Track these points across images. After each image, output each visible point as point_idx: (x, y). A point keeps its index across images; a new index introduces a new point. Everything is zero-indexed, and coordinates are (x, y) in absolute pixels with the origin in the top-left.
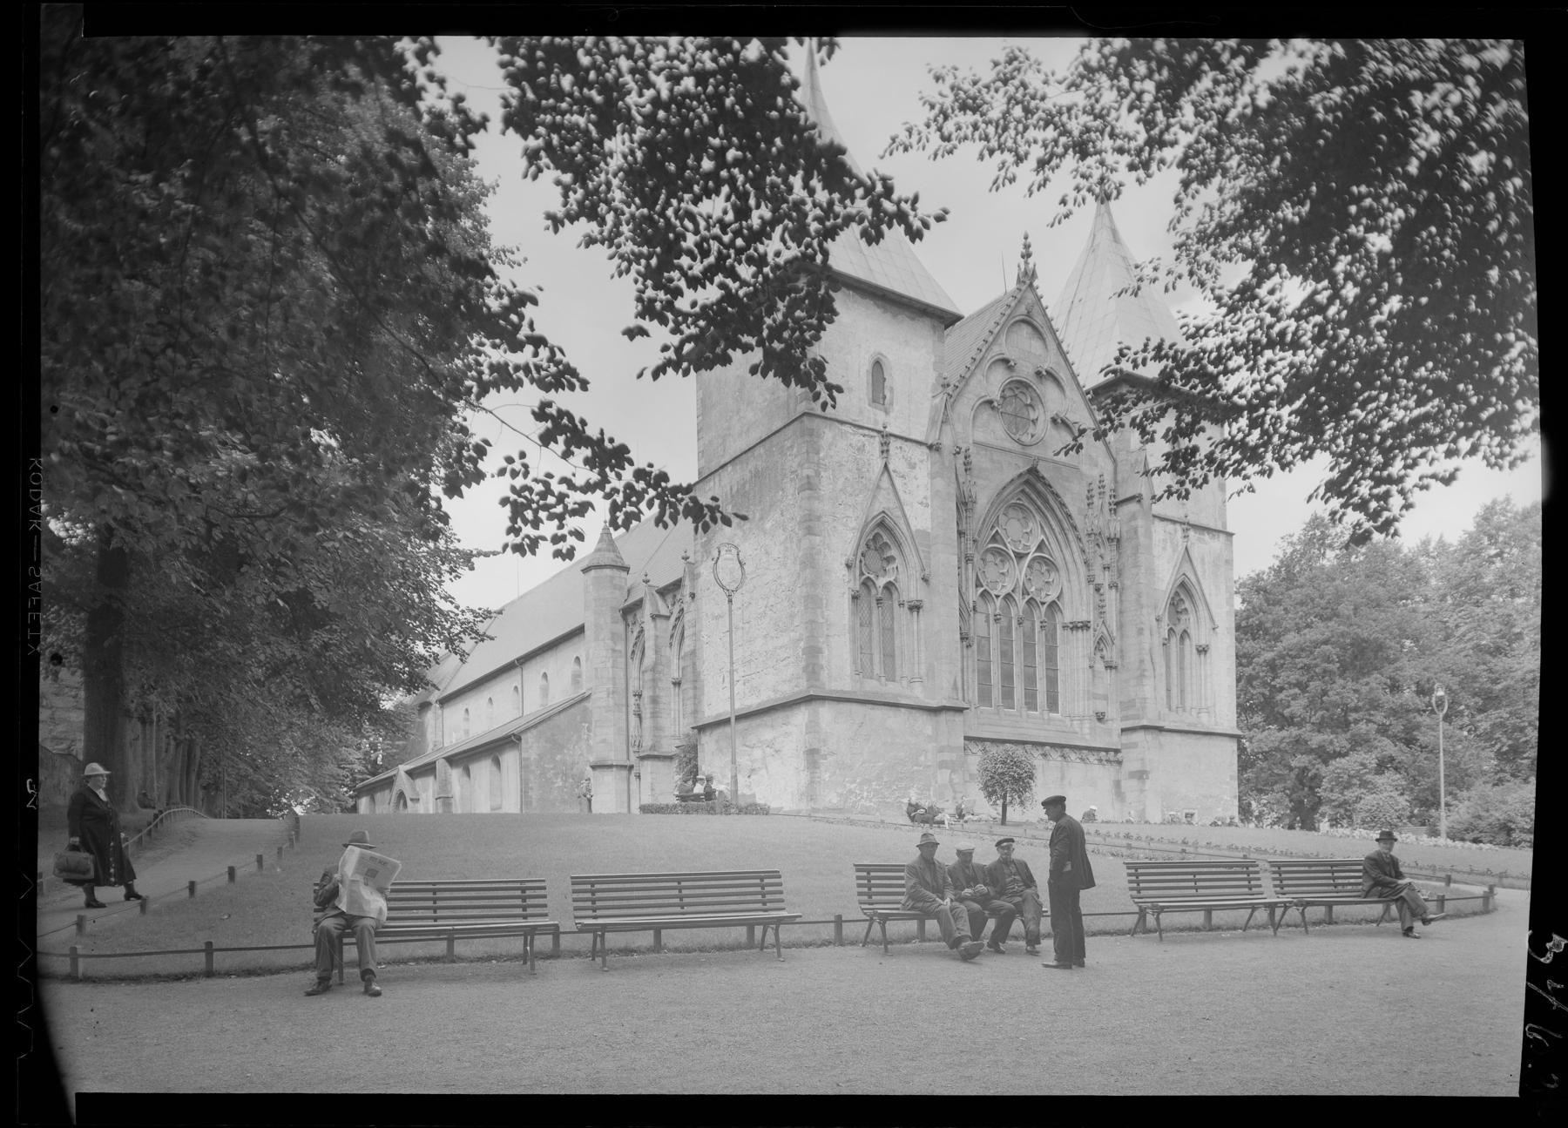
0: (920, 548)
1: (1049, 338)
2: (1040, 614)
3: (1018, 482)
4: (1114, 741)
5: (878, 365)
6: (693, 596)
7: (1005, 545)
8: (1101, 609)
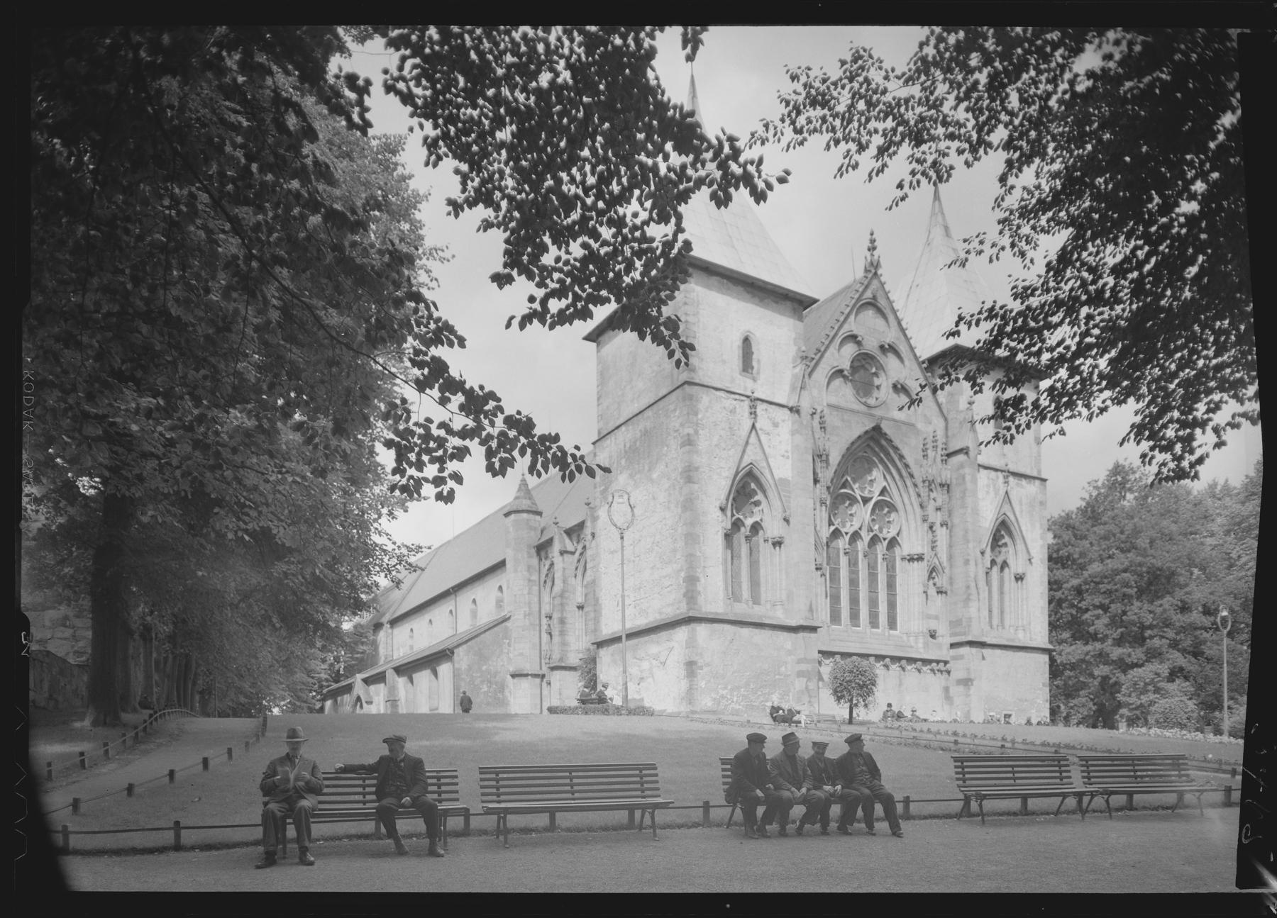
0: (782, 493)
2: (881, 549)
3: (863, 440)
4: (945, 653)
5: (746, 341)
6: (593, 535)
7: (853, 490)
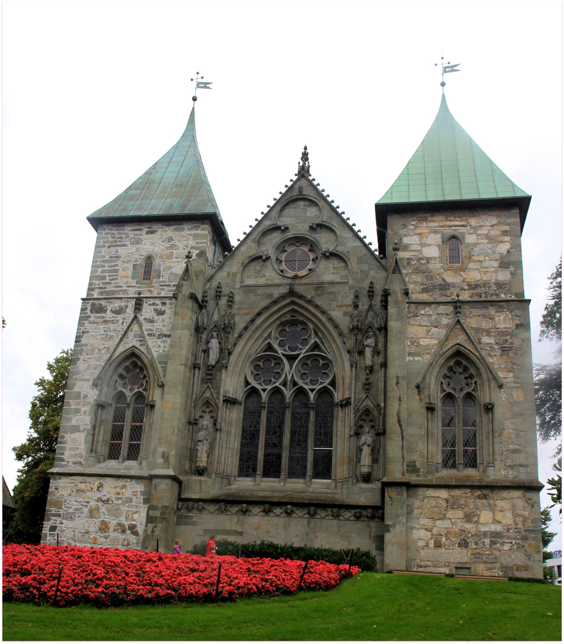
1: (321, 203)
8: (368, 386)
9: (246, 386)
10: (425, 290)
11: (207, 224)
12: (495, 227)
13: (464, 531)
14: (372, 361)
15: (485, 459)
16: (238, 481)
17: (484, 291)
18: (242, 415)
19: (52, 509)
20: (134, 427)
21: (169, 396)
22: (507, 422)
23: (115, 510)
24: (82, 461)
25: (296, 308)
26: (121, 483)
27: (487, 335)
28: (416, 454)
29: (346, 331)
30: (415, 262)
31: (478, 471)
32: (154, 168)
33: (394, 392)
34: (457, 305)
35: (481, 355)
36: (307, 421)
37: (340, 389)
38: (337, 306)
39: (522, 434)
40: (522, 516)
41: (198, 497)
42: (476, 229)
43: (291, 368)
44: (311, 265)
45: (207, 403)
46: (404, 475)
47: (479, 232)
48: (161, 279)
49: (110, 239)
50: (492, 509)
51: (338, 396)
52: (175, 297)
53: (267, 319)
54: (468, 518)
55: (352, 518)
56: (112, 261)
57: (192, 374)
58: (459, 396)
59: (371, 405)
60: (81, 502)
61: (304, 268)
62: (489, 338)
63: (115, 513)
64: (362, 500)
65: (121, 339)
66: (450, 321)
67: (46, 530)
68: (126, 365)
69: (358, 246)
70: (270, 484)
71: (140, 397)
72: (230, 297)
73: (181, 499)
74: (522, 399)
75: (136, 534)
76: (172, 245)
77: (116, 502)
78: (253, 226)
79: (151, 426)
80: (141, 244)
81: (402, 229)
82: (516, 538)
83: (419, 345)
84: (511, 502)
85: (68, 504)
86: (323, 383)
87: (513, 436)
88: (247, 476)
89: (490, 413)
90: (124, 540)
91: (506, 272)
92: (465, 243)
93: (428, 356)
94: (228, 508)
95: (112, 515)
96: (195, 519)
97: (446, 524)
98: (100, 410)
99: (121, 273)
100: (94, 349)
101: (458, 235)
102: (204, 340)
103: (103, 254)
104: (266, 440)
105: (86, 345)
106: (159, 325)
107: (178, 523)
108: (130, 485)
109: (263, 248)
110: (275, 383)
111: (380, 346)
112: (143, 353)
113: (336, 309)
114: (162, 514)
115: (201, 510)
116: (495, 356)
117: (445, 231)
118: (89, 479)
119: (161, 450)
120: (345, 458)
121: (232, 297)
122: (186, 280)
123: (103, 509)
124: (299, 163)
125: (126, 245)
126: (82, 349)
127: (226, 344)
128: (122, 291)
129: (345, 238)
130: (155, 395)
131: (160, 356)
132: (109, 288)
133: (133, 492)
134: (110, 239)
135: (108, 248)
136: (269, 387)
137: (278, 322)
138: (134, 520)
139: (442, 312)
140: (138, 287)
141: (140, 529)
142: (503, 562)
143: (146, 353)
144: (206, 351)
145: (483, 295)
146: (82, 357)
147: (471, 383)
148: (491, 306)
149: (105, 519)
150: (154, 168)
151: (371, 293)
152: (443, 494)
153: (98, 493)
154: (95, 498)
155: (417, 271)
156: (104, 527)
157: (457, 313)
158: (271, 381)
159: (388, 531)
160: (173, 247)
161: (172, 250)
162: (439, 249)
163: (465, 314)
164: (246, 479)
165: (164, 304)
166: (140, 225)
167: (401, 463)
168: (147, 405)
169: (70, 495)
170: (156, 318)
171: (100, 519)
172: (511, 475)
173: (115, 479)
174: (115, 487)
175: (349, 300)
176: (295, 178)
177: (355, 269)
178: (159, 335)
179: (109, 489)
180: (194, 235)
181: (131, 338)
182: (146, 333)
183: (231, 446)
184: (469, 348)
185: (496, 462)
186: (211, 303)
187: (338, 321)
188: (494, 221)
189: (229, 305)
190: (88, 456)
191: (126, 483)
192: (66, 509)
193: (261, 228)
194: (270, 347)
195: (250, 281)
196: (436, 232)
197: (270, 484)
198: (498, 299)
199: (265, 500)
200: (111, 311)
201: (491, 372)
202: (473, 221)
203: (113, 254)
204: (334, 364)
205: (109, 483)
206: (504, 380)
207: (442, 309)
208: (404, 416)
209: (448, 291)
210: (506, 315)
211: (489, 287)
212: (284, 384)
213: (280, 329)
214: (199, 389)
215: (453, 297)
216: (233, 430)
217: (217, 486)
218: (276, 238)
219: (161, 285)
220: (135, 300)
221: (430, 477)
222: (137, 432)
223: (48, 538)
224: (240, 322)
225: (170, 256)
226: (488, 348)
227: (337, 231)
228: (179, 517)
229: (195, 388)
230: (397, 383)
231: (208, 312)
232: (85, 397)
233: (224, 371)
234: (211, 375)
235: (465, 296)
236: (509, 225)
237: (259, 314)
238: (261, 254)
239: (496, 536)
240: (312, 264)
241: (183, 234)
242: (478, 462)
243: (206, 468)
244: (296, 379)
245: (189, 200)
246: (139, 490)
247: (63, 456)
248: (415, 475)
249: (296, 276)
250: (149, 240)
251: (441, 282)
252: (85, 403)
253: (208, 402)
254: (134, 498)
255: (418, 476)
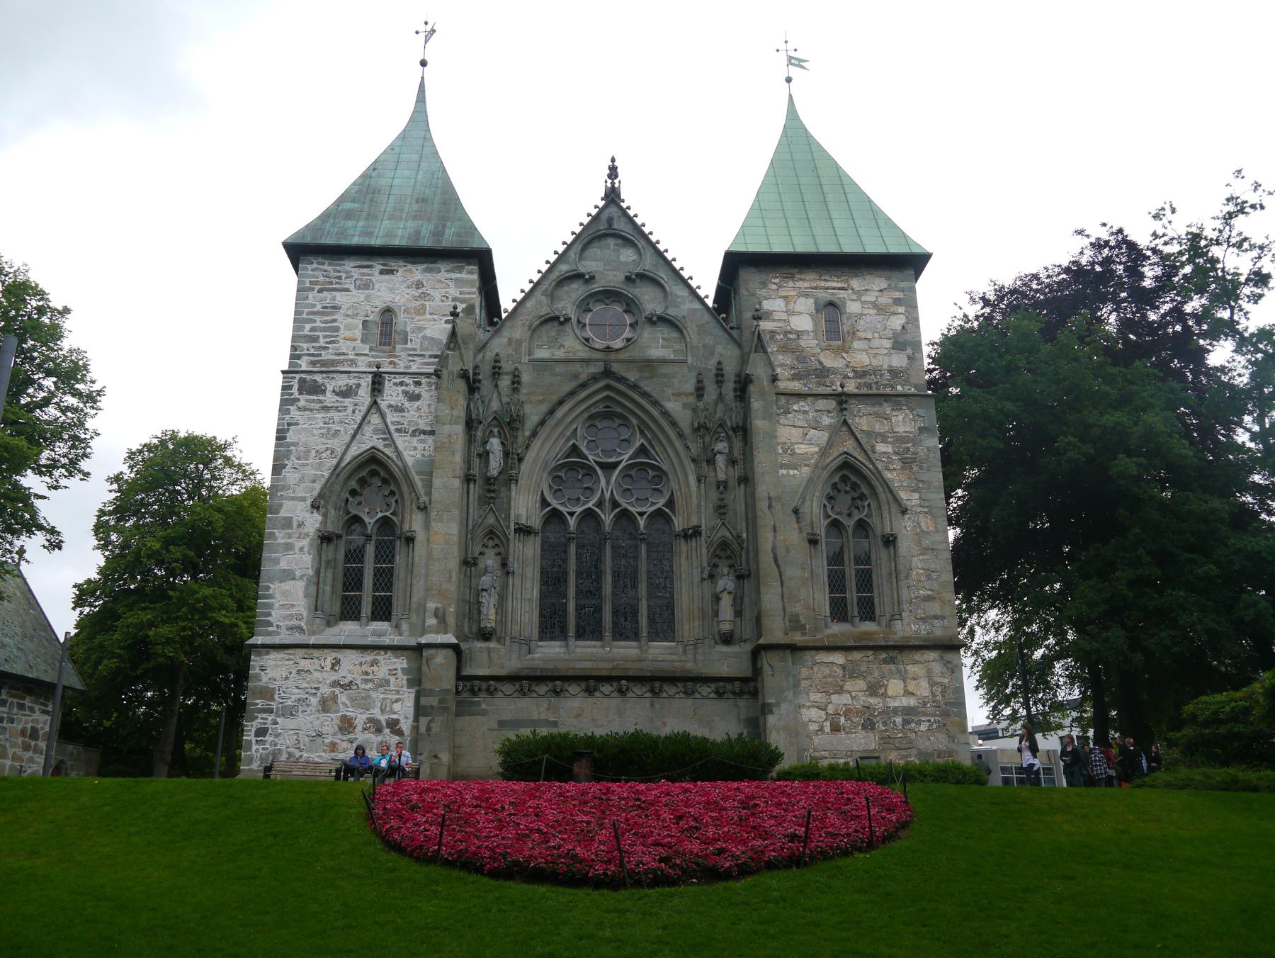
8: (721, 509)
9: (542, 509)
10: (795, 377)
11: (475, 265)
12: (885, 293)
13: (869, 708)
14: (726, 474)
15: (888, 609)
16: (541, 647)
17: (875, 380)
18: (539, 551)
19: (258, 701)
20: (378, 571)
21: (439, 524)
22: (915, 559)
23: (363, 698)
24: (303, 624)
25: (612, 394)
26: (369, 657)
27: (882, 442)
28: (797, 605)
29: (687, 431)
30: (782, 336)
31: (879, 625)
32: (374, 169)
33: (766, 519)
34: (842, 399)
35: (877, 469)
36: (636, 558)
37: (681, 512)
38: (673, 394)
39: (935, 576)
40: (941, 684)
41: (487, 674)
42: (859, 294)
43: (608, 482)
44: (627, 333)
45: (491, 533)
46: (787, 634)
47: (863, 299)
48: (409, 345)
49: (321, 279)
50: (903, 676)
51: (679, 523)
52: (437, 374)
53: (571, 409)
54: (873, 690)
55: (712, 695)
56: (327, 314)
57: (465, 490)
58: (850, 523)
59: (729, 535)
60: (306, 688)
61: (618, 337)
62: (886, 445)
63: (364, 703)
64: (725, 669)
65: (354, 436)
66: (833, 421)
67: (250, 735)
68: (361, 475)
69: (698, 309)
70: (589, 650)
71: (386, 525)
72: (515, 376)
73: (460, 677)
74: (931, 528)
75: (399, 733)
76: (423, 293)
77: (363, 686)
78: (543, 271)
79: (410, 569)
80: (373, 289)
81: (760, 289)
82: (934, 715)
83: (793, 454)
84: (926, 667)
85: (284, 692)
86: (656, 503)
87: (923, 578)
88: (552, 639)
89: (892, 547)
90: (381, 743)
91: (901, 356)
92: (846, 313)
93: (807, 468)
94: (534, 688)
95: (359, 706)
96: (484, 706)
97: (844, 699)
98: (325, 545)
99: (343, 333)
100: (309, 451)
101: (835, 300)
102: (479, 439)
103: (310, 301)
104: (577, 587)
105: (295, 444)
106: (413, 416)
107: (457, 715)
108: (385, 659)
109: (559, 305)
110: (588, 502)
111: (737, 453)
112: (389, 457)
113: (672, 399)
114: (440, 701)
115: (491, 692)
116: (895, 469)
117: (820, 295)
118: (316, 653)
119: (431, 605)
120: (696, 611)
121: (518, 376)
122: (453, 350)
123: (343, 698)
124: (606, 182)
125: (347, 290)
126: (288, 451)
127: (515, 447)
128: (347, 361)
129: (678, 297)
130: (416, 523)
131: (418, 462)
132: (325, 356)
133: (390, 670)
134: (321, 279)
135: (318, 292)
136: (579, 510)
137: (586, 415)
138: (395, 713)
139: (822, 408)
140: (373, 357)
141: (406, 726)
142: (921, 747)
143: (395, 458)
144: (485, 456)
145: (874, 386)
146: (289, 464)
147: (864, 507)
148: (886, 401)
149: (348, 714)
150: (374, 169)
151: (719, 377)
152: (838, 658)
153: (334, 673)
154: (328, 682)
155: (785, 349)
156: (347, 725)
157: (842, 410)
158: (578, 499)
159: (771, 712)
160: (424, 296)
161: (423, 302)
162: (812, 319)
163: (852, 412)
164: (552, 643)
165: (418, 384)
166: (369, 260)
167: (782, 618)
168: (400, 538)
169: (287, 678)
170: (407, 405)
171: (340, 714)
172: (924, 630)
173: (359, 651)
174: (361, 664)
175: (690, 386)
176: (601, 204)
177: (695, 342)
178: (414, 431)
179: (352, 667)
180: (457, 280)
181: (368, 434)
182: (392, 428)
183: (528, 596)
184: (860, 459)
185: (903, 614)
186: (486, 385)
187: (674, 415)
188: (883, 283)
189: (514, 389)
190: (310, 616)
191: (377, 657)
192: (281, 701)
193: (555, 275)
194: (575, 450)
195: (542, 353)
196: (807, 296)
197: (589, 650)
198: (892, 393)
199: (588, 674)
200: (333, 391)
201: (891, 491)
202: (856, 283)
203: (328, 302)
204: (671, 477)
205: (349, 658)
206: (908, 503)
207: (821, 404)
208: (781, 552)
209: (827, 379)
210: (906, 414)
211: (881, 375)
212: (600, 504)
213: (587, 425)
214: (476, 513)
215: (834, 388)
216: (530, 574)
217: (514, 656)
218: (576, 291)
219: (410, 355)
220: (370, 376)
221: (819, 636)
222: (385, 579)
223: (254, 748)
224: (533, 414)
225: (421, 311)
226: (885, 459)
227: (665, 285)
228: (459, 704)
229: (471, 510)
230: (770, 507)
231: (481, 397)
232: (300, 525)
233: (513, 486)
234: (494, 491)
235: (851, 387)
236: (903, 291)
237: (561, 403)
238: (557, 313)
239: (908, 712)
240: (630, 331)
241: (438, 278)
242: (877, 612)
243: (494, 630)
244: (617, 498)
245: (444, 226)
246: (399, 667)
247: (269, 618)
248: (799, 633)
249: (608, 347)
250: (385, 284)
251: (816, 365)
252: (300, 534)
253: (491, 532)
254: (392, 679)
255: (804, 634)
